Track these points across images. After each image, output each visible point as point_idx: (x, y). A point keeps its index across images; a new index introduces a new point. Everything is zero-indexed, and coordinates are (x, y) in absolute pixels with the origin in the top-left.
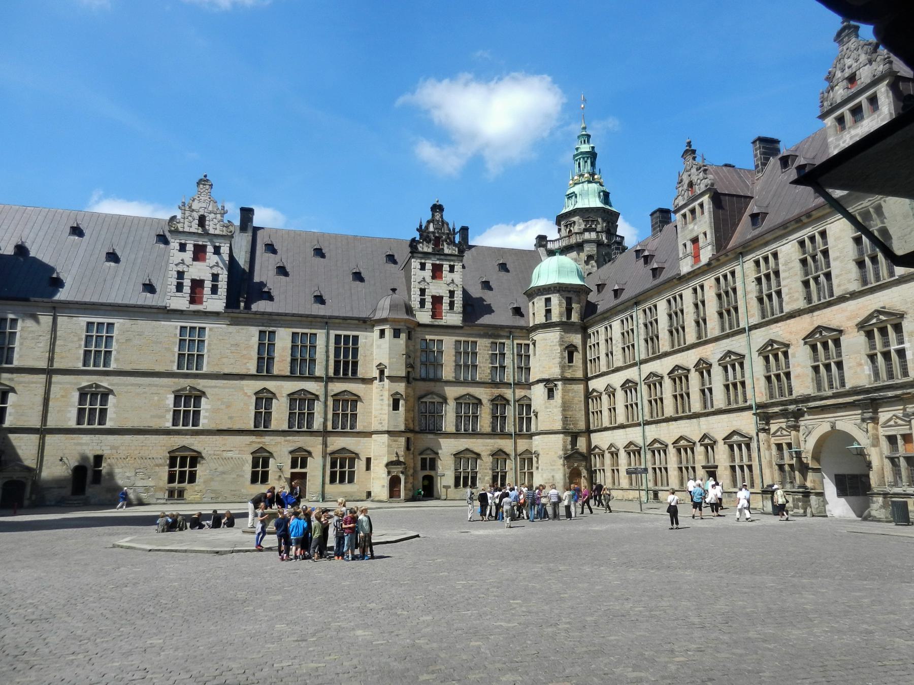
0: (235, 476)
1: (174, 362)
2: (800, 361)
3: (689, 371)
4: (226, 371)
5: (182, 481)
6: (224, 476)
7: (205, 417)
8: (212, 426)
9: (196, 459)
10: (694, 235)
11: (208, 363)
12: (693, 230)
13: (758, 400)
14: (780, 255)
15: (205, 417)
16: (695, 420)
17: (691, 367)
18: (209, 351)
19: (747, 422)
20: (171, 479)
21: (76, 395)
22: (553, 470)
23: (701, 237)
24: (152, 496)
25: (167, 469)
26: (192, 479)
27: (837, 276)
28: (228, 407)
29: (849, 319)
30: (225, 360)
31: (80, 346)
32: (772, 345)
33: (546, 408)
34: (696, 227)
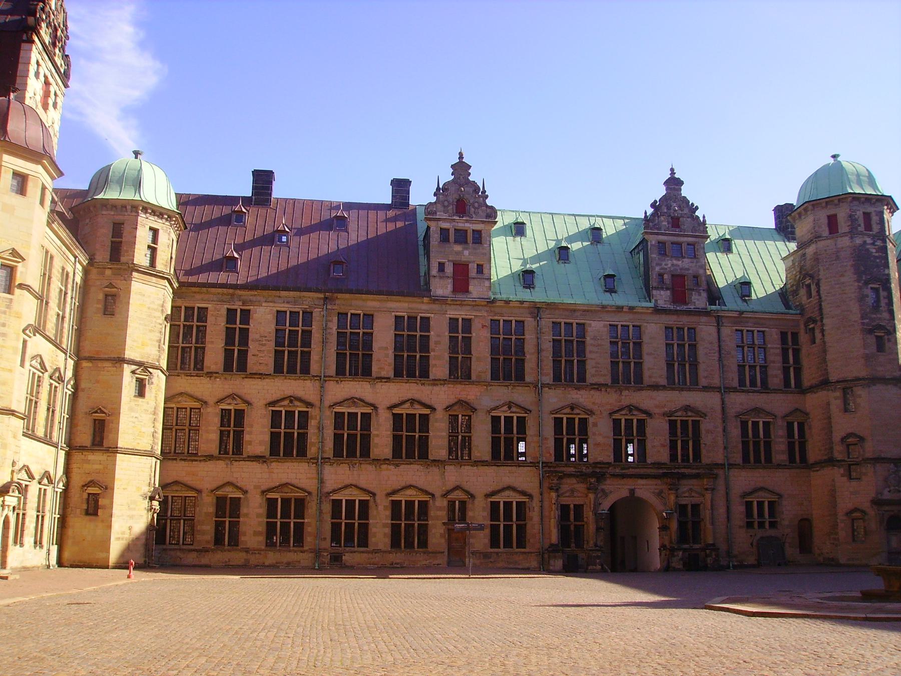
2: (601, 432)
3: (433, 409)
10: (464, 259)
12: (458, 253)
13: (544, 460)
14: (589, 329)
16: (435, 470)
17: (440, 408)
19: (524, 479)
22: (131, 517)
23: (473, 268)
27: (649, 369)
29: (657, 407)
32: (572, 409)
33: (131, 409)
34: (466, 253)
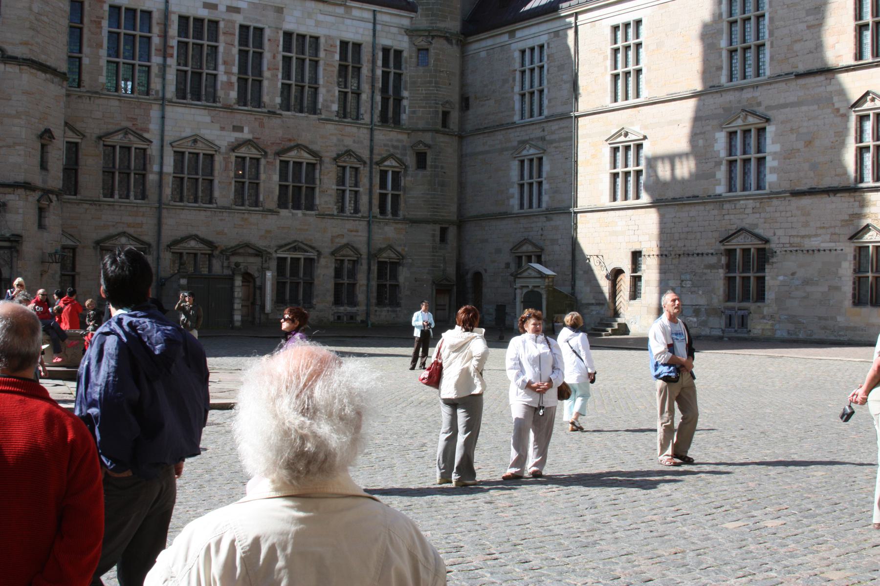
0: (826, 289)
1: (720, 68)
4: (801, 69)
5: (745, 297)
6: (809, 289)
7: (773, 170)
8: (786, 186)
9: (763, 257)
11: (772, 58)
15: (773, 170)
18: (771, 34)
20: (730, 296)
21: (607, 151)
24: (704, 324)
25: (721, 272)
26: (761, 296)
28: (809, 144)
30: (797, 47)
31: (606, 67)
